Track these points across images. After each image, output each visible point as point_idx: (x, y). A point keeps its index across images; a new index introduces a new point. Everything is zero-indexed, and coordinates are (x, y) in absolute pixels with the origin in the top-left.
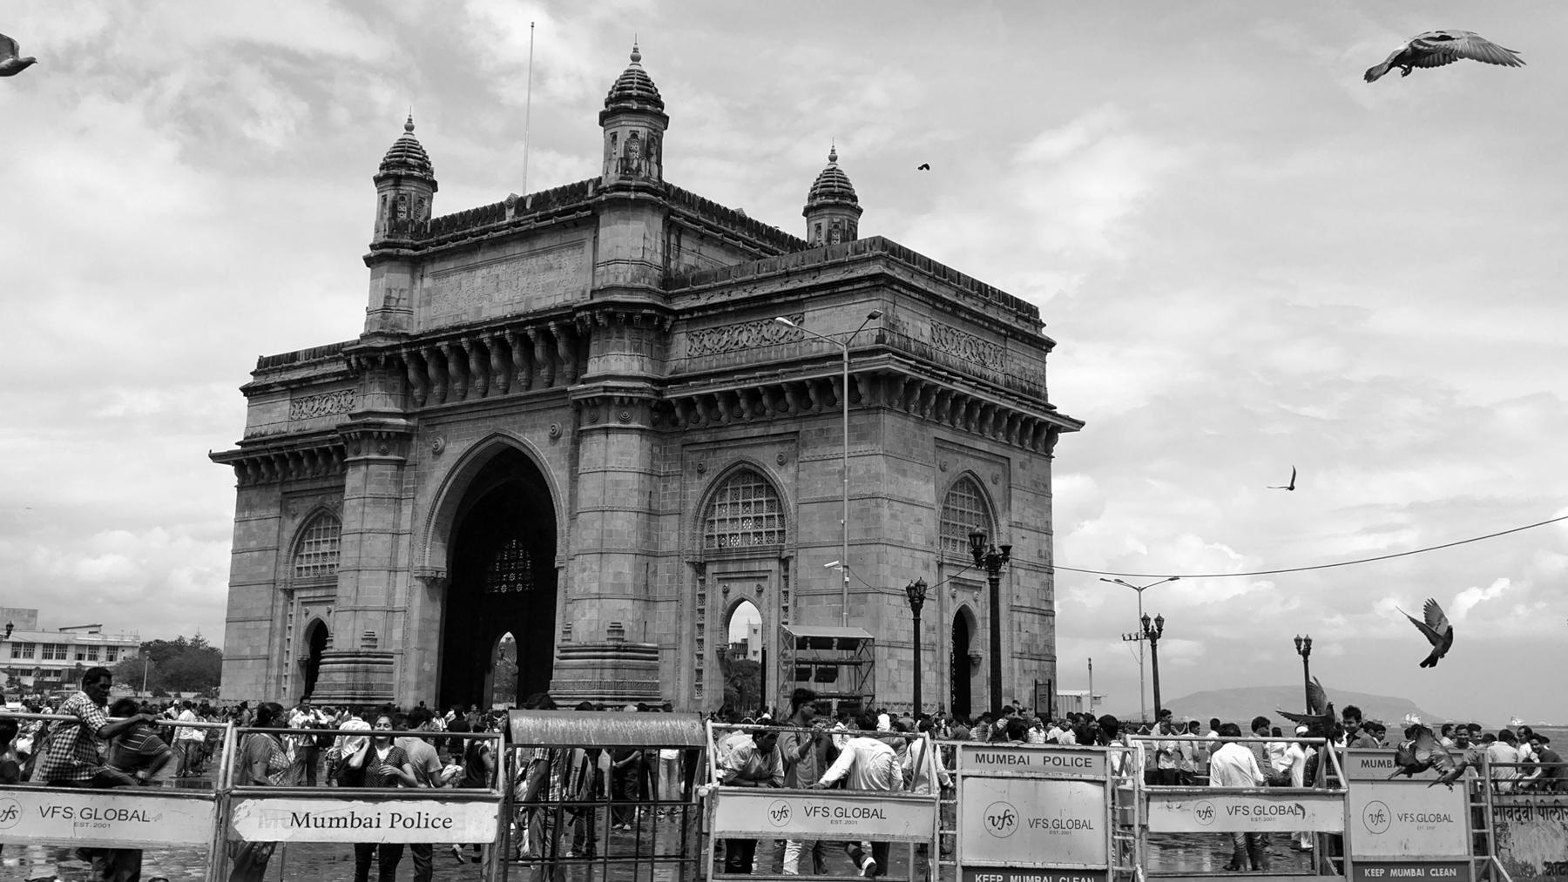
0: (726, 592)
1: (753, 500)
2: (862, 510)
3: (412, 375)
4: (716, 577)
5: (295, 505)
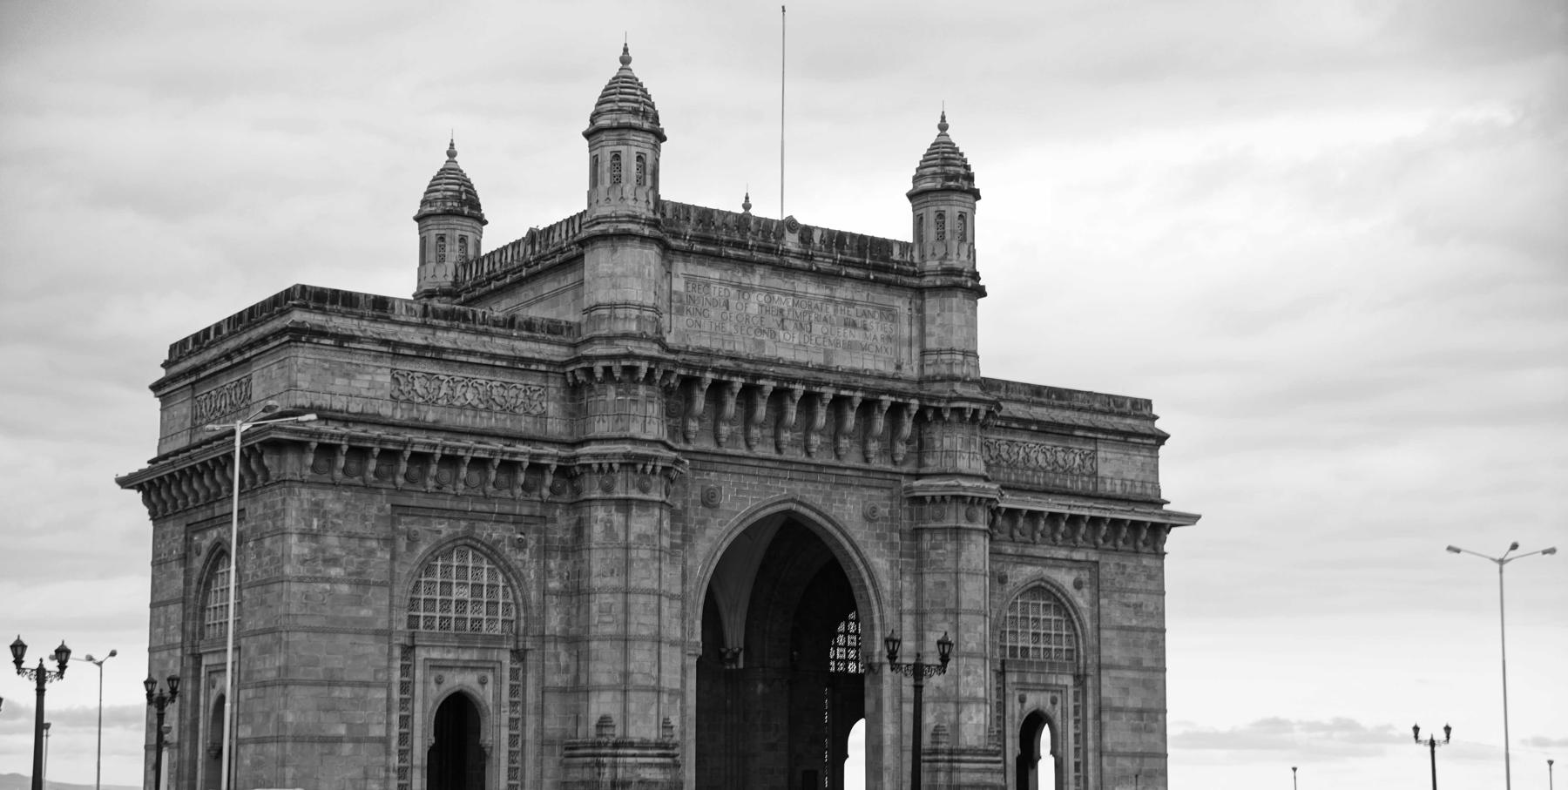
0: (1022, 700)
1: (1042, 617)
2: (1153, 642)
3: (700, 402)
4: (1015, 687)
5: (404, 524)
